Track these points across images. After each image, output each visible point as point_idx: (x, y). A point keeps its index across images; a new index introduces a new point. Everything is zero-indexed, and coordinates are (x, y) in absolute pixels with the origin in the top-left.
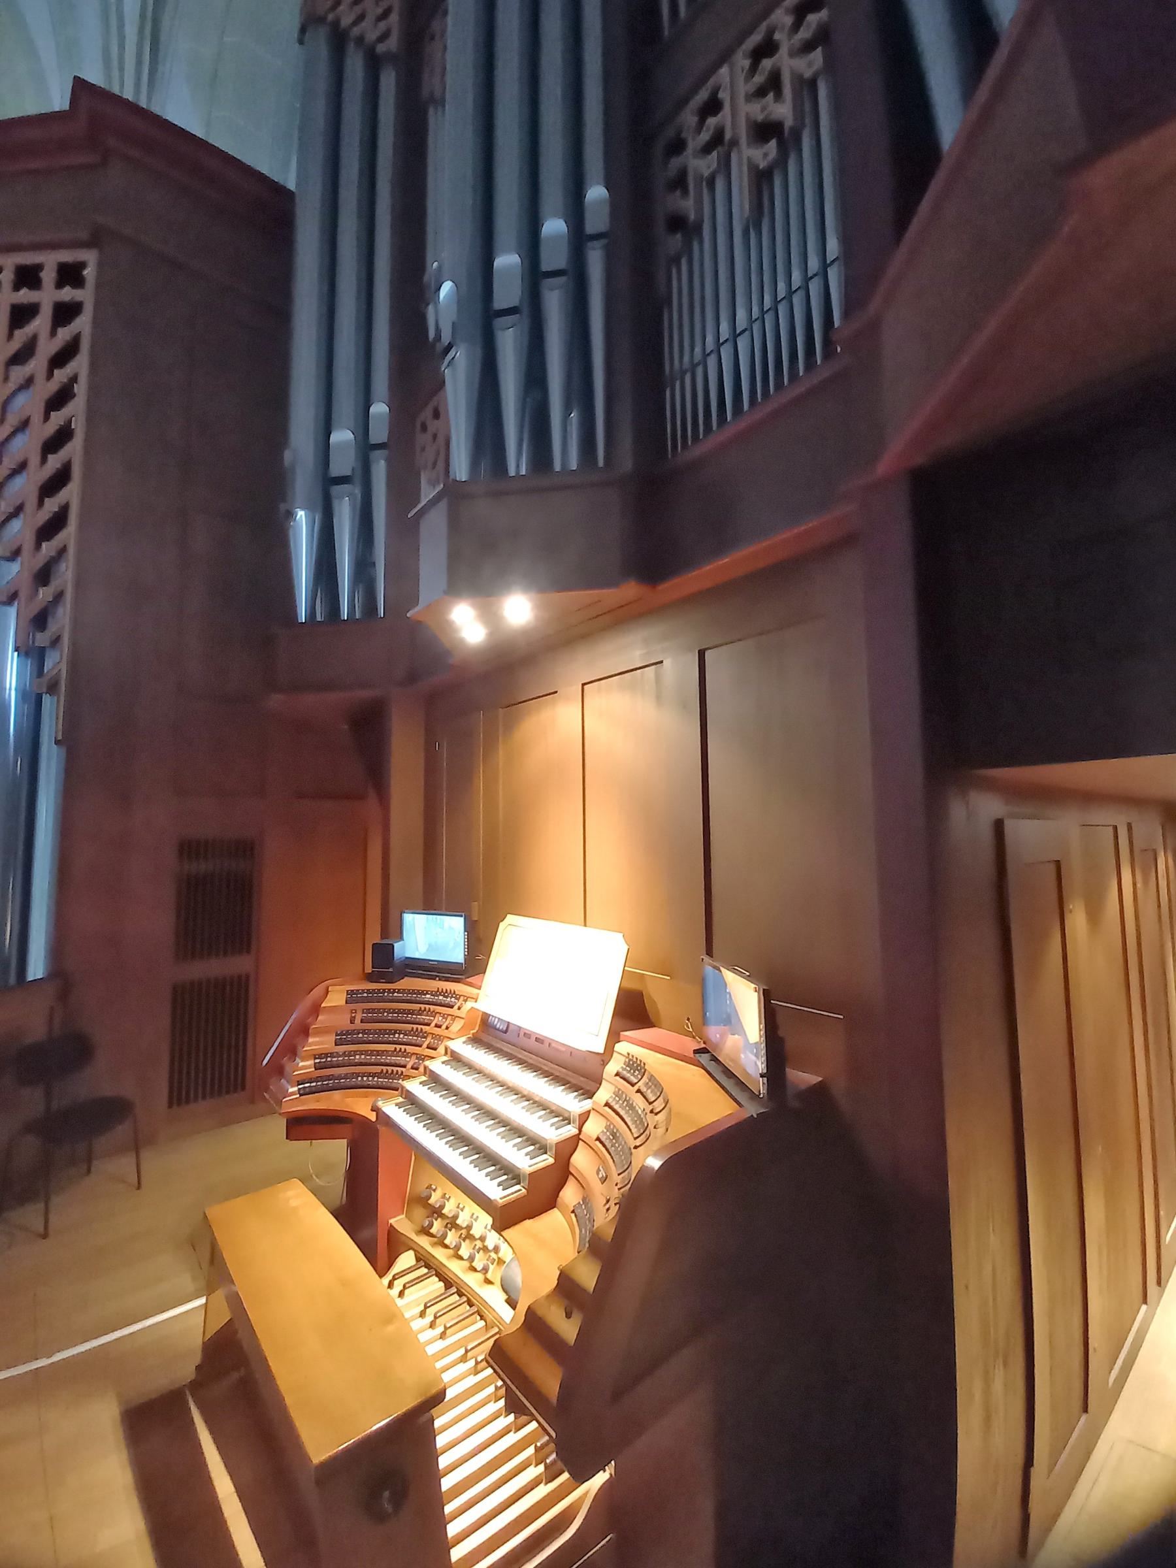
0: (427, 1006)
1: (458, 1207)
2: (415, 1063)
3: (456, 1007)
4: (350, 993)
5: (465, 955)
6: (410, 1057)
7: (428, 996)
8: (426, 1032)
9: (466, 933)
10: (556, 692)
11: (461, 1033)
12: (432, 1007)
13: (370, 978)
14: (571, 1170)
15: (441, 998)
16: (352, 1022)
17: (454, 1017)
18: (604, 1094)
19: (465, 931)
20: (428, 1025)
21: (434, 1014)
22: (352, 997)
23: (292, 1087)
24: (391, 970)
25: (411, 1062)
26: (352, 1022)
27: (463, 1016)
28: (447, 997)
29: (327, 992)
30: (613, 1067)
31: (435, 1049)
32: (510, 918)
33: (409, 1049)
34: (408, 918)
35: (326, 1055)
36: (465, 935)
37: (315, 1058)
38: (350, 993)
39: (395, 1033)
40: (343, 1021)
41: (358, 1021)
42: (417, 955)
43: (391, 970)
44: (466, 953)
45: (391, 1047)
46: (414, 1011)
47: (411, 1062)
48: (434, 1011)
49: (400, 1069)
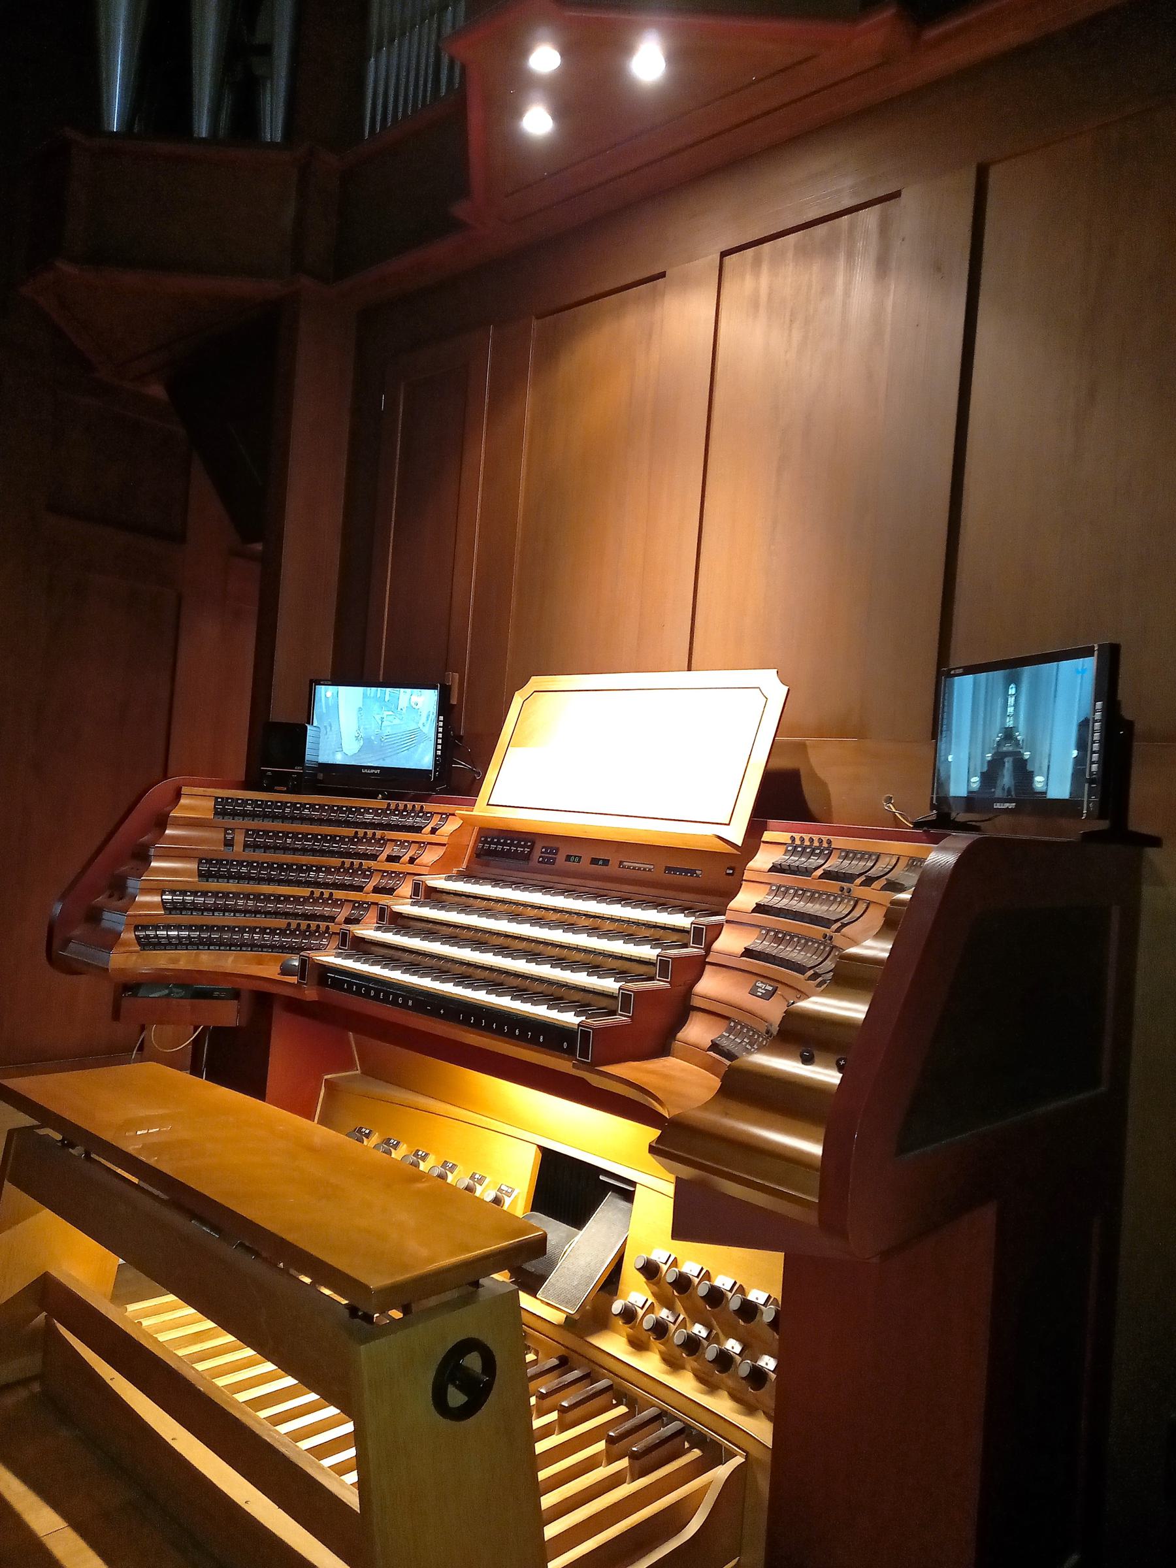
0: (370, 832)
1: (416, 1154)
2: (351, 914)
3: (428, 829)
4: (221, 802)
5: (436, 756)
6: (341, 906)
7: (367, 816)
8: (369, 869)
9: (441, 718)
10: (663, 275)
11: (439, 867)
12: (379, 833)
13: (249, 784)
14: (696, 1002)
15: (394, 818)
16: (229, 843)
17: (422, 845)
18: (745, 899)
19: (439, 714)
20: (374, 857)
21: (382, 842)
22: (223, 809)
23: (127, 930)
24: (298, 770)
25: (343, 913)
26: (229, 843)
27: (444, 840)
28: (408, 815)
29: (178, 795)
30: (763, 860)
31: (390, 891)
32: (536, 682)
33: (339, 894)
34: (325, 693)
35: (183, 893)
36: (438, 721)
37: (163, 893)
38: (221, 802)
39: (309, 869)
40: (211, 840)
41: (238, 848)
42: (339, 759)
43: (298, 770)
44: (439, 753)
45: (305, 892)
46: (342, 838)
47: (343, 913)
48: (382, 838)
49: (323, 925)
